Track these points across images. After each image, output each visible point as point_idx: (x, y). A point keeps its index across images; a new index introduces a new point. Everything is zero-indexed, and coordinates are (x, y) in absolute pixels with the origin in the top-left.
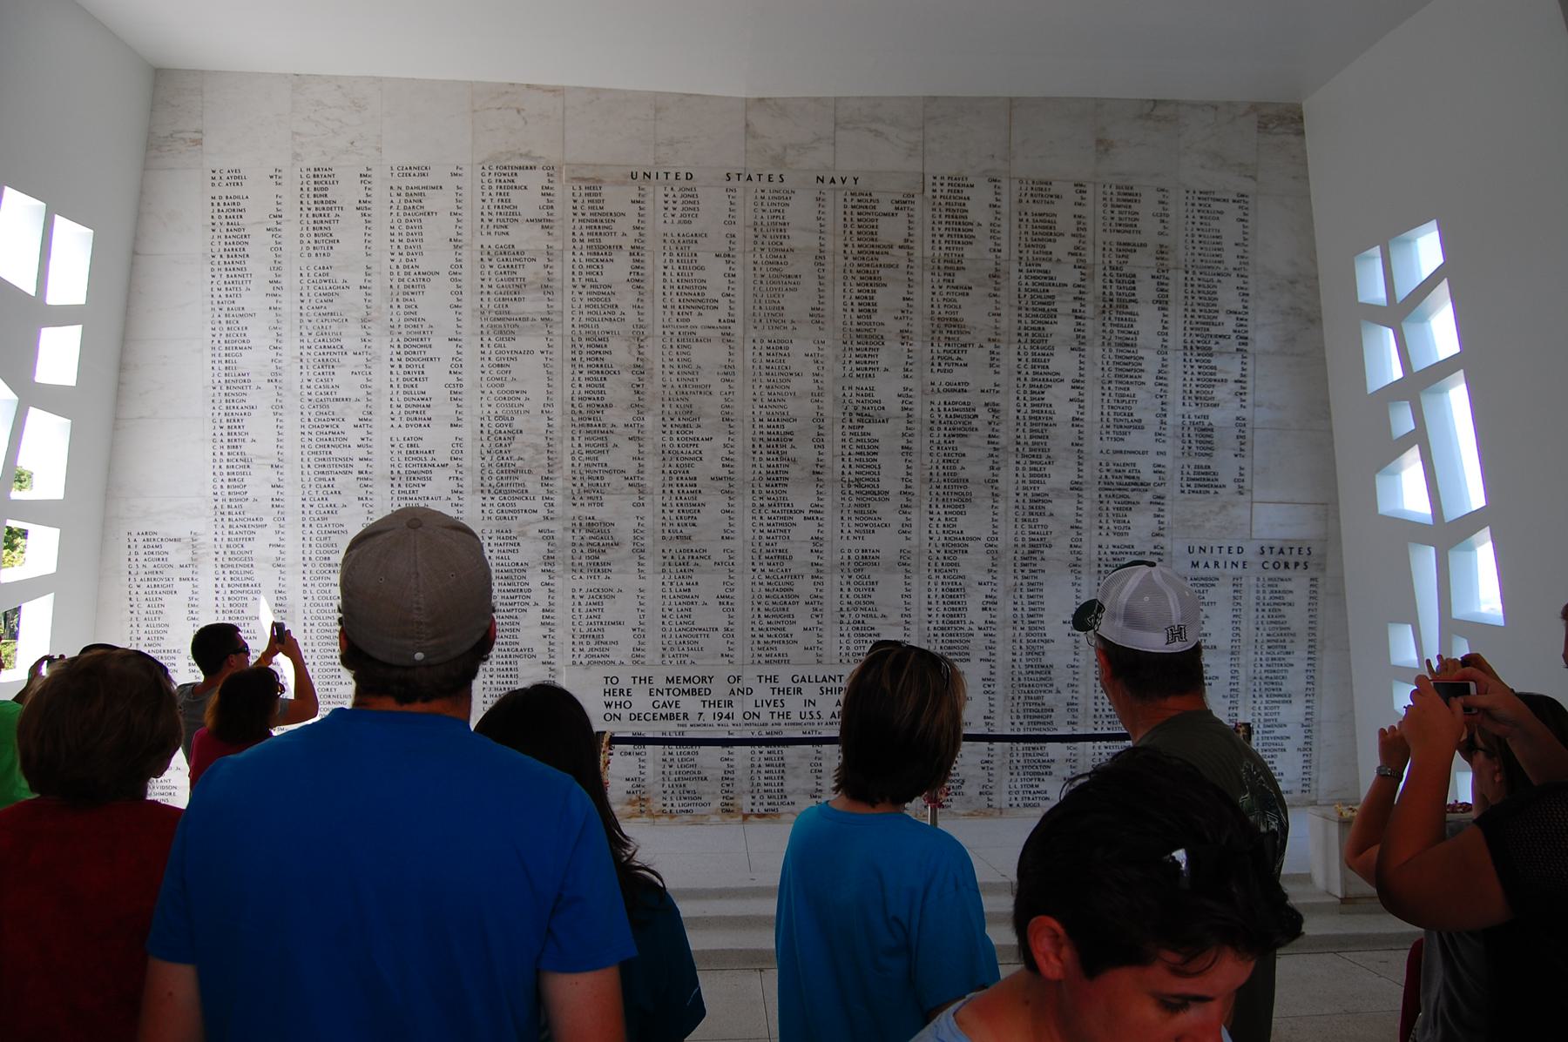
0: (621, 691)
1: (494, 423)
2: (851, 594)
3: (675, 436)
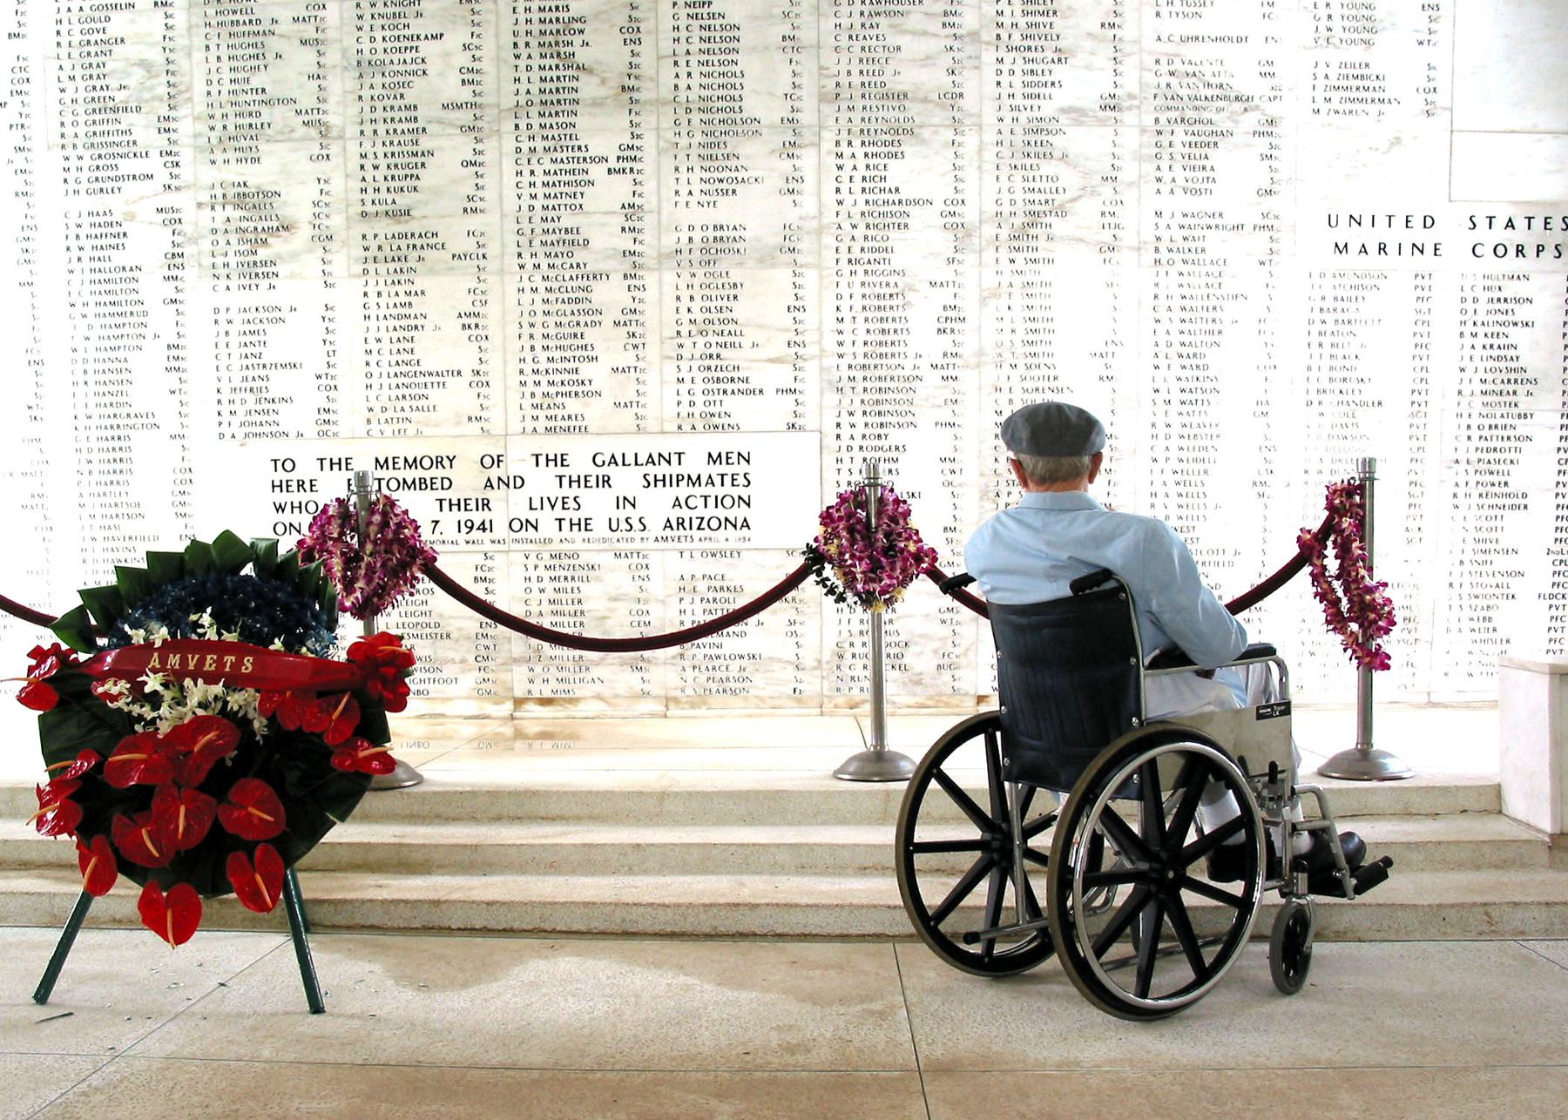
0: (301, 484)
1: (77, 27)
2: (696, 306)
3: (379, 35)
